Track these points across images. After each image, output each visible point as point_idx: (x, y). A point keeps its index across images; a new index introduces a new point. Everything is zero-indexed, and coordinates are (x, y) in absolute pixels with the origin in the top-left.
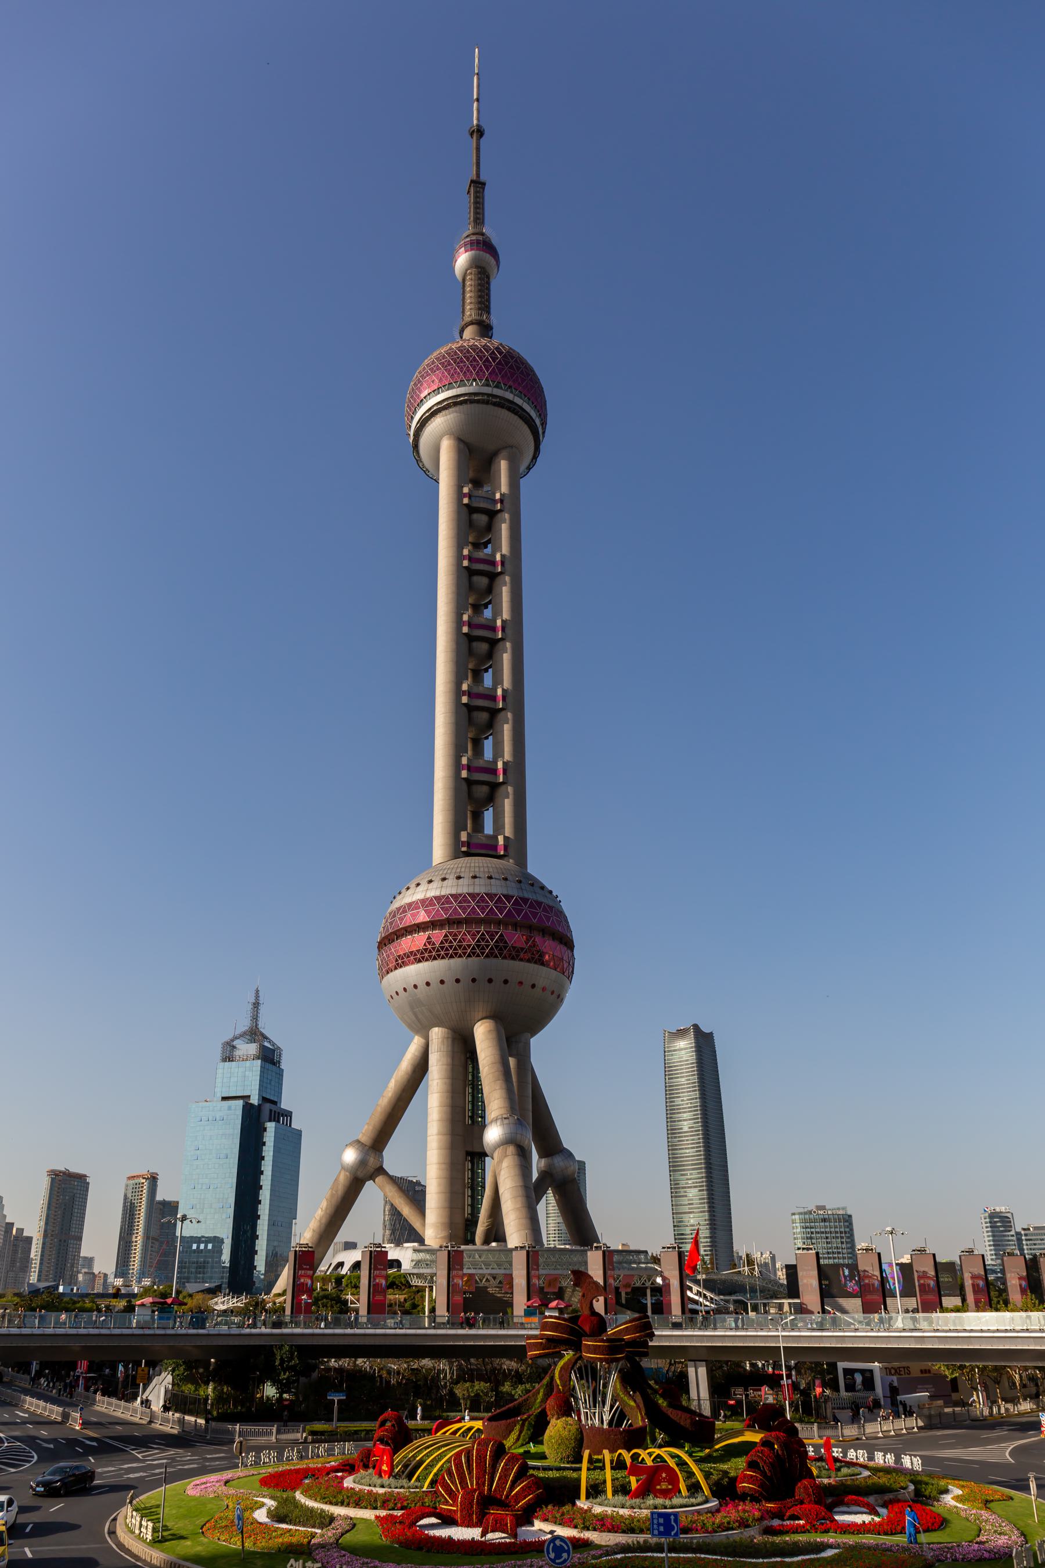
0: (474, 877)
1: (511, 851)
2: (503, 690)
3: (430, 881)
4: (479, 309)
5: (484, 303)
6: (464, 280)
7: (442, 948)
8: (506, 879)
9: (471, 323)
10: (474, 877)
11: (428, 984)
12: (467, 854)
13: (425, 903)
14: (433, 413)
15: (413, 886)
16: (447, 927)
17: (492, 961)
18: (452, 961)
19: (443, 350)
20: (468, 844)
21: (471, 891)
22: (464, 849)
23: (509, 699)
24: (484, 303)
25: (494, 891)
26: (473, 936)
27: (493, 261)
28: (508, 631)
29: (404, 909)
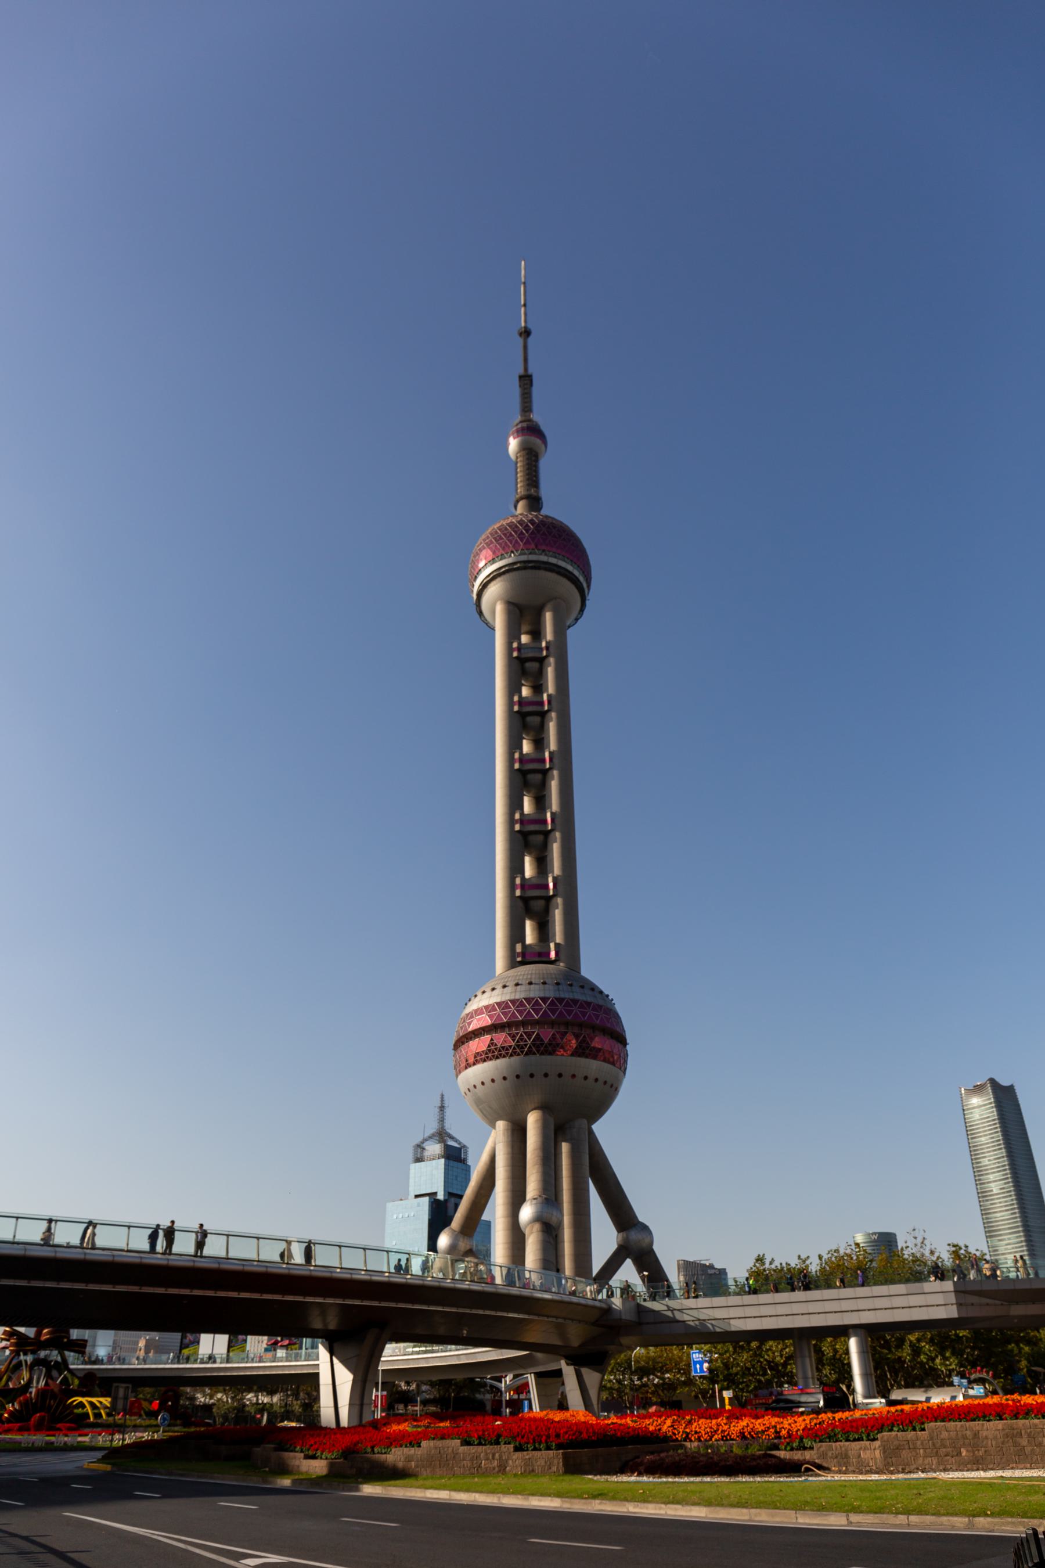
0: (530, 983)
1: (562, 956)
2: (552, 813)
3: (493, 989)
4: (528, 485)
5: (532, 478)
6: (516, 463)
7: (503, 1048)
8: (544, 983)
9: (521, 498)
10: (517, 985)
11: (493, 1081)
12: (523, 963)
13: (489, 1009)
14: (484, 586)
15: (479, 993)
16: (507, 1029)
17: (532, 1058)
18: (512, 1059)
19: (490, 530)
20: (523, 954)
21: (542, 995)
22: (519, 959)
23: (557, 821)
24: (532, 478)
25: (547, 995)
26: (513, 1037)
27: (538, 441)
28: (555, 761)
29: (471, 1016)
